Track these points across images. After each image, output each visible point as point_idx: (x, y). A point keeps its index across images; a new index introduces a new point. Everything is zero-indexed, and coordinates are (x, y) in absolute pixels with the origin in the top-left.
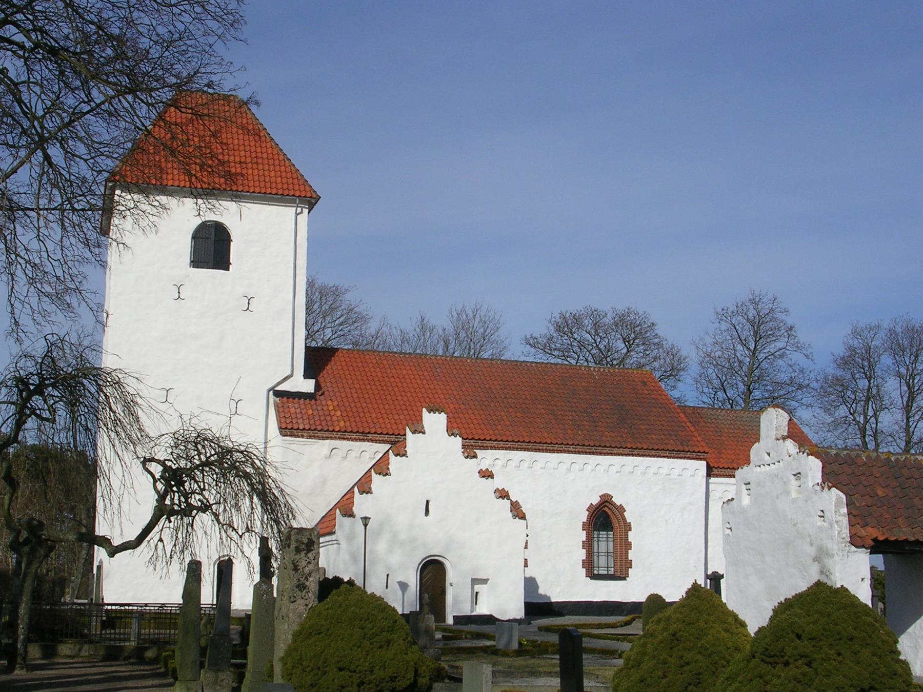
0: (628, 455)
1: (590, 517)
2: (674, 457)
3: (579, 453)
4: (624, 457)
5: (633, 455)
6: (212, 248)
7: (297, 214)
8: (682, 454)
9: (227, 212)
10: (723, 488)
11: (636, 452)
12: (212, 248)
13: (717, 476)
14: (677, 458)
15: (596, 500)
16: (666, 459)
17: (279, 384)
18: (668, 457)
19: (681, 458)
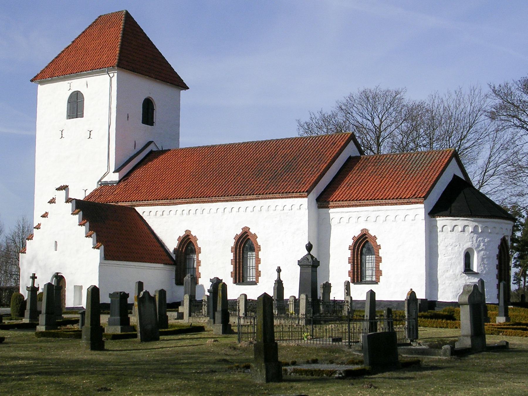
0: (256, 199)
1: (236, 244)
2: (285, 198)
3: (227, 201)
4: (255, 201)
5: (259, 199)
6: (76, 106)
7: (111, 78)
8: (290, 195)
9: (77, 84)
10: (339, 215)
11: (260, 196)
12: (76, 106)
13: (334, 207)
14: (288, 198)
15: (239, 232)
16: (281, 200)
17: (102, 178)
18: (282, 198)
19: (290, 197)
